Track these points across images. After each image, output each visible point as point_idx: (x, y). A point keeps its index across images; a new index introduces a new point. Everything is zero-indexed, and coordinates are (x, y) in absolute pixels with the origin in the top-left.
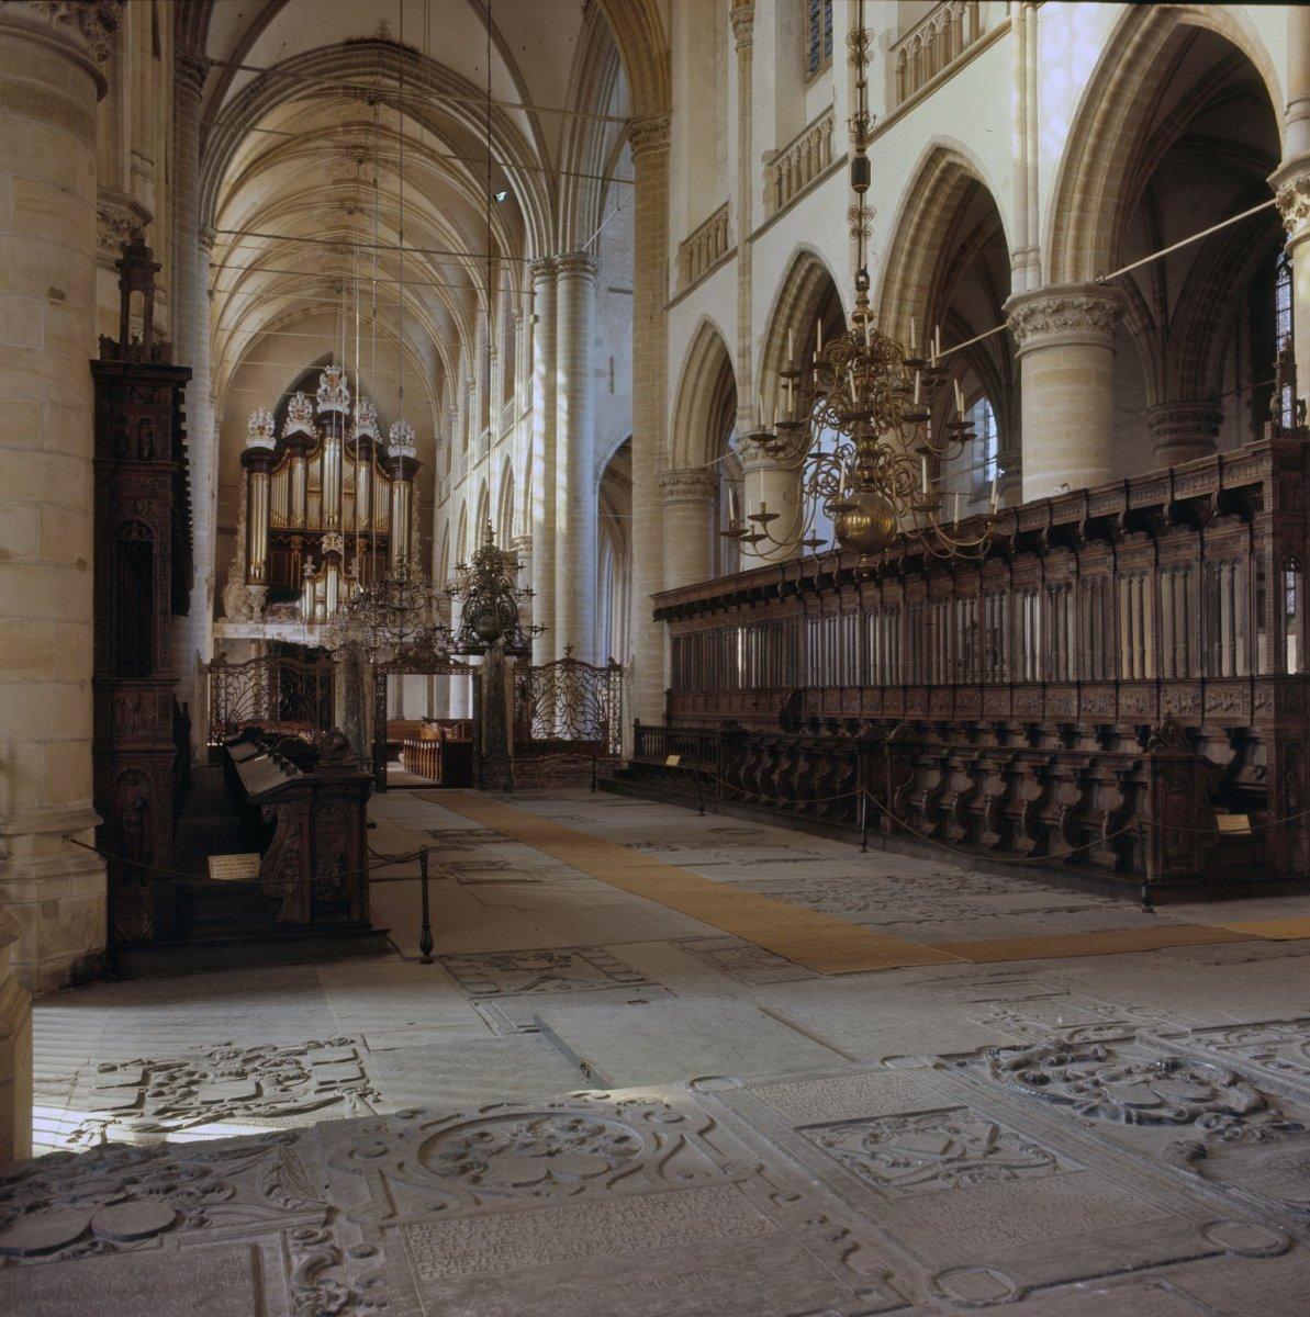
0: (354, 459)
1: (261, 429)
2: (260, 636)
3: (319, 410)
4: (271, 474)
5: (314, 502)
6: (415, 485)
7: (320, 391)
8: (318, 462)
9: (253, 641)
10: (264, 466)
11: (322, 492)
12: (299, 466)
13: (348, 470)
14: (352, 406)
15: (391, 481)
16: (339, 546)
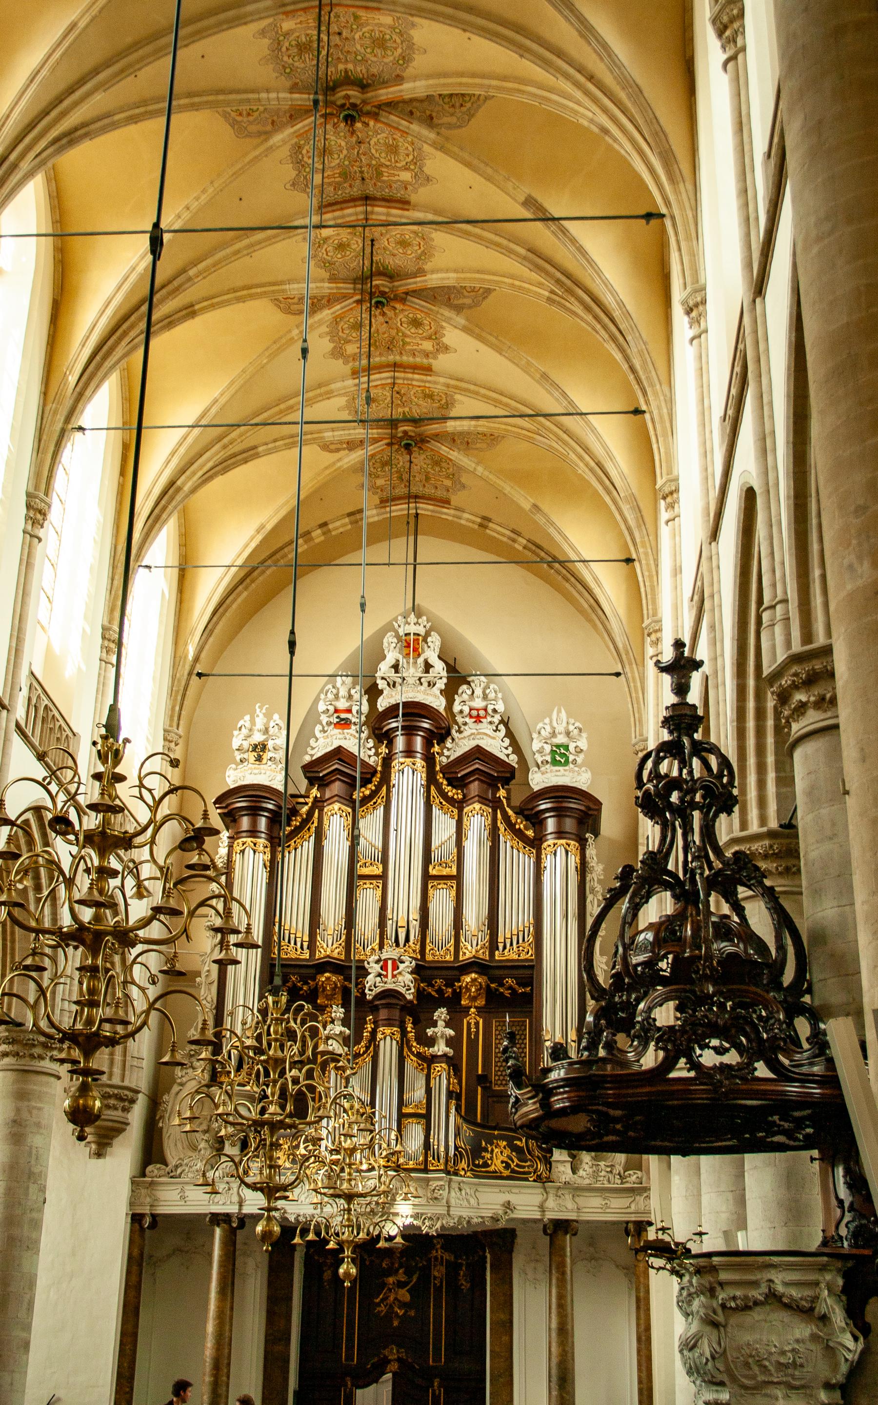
0: (451, 801)
1: (260, 749)
2: (233, 1209)
3: (383, 704)
4: (276, 842)
5: (368, 899)
6: (591, 852)
7: (384, 668)
8: (380, 811)
9: (217, 1219)
10: (263, 823)
11: (383, 877)
12: (336, 822)
13: (444, 827)
14: (450, 693)
15: (536, 844)
16: (404, 981)
